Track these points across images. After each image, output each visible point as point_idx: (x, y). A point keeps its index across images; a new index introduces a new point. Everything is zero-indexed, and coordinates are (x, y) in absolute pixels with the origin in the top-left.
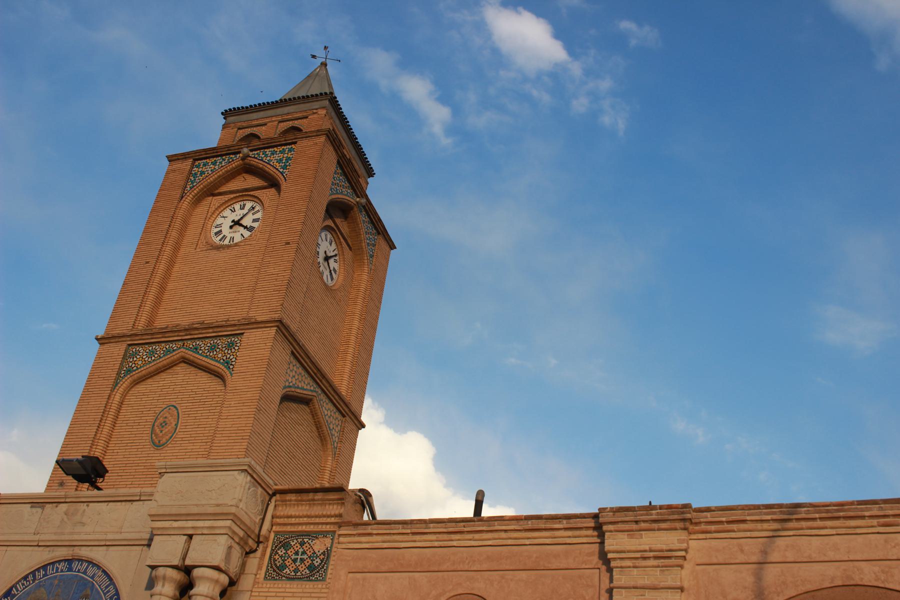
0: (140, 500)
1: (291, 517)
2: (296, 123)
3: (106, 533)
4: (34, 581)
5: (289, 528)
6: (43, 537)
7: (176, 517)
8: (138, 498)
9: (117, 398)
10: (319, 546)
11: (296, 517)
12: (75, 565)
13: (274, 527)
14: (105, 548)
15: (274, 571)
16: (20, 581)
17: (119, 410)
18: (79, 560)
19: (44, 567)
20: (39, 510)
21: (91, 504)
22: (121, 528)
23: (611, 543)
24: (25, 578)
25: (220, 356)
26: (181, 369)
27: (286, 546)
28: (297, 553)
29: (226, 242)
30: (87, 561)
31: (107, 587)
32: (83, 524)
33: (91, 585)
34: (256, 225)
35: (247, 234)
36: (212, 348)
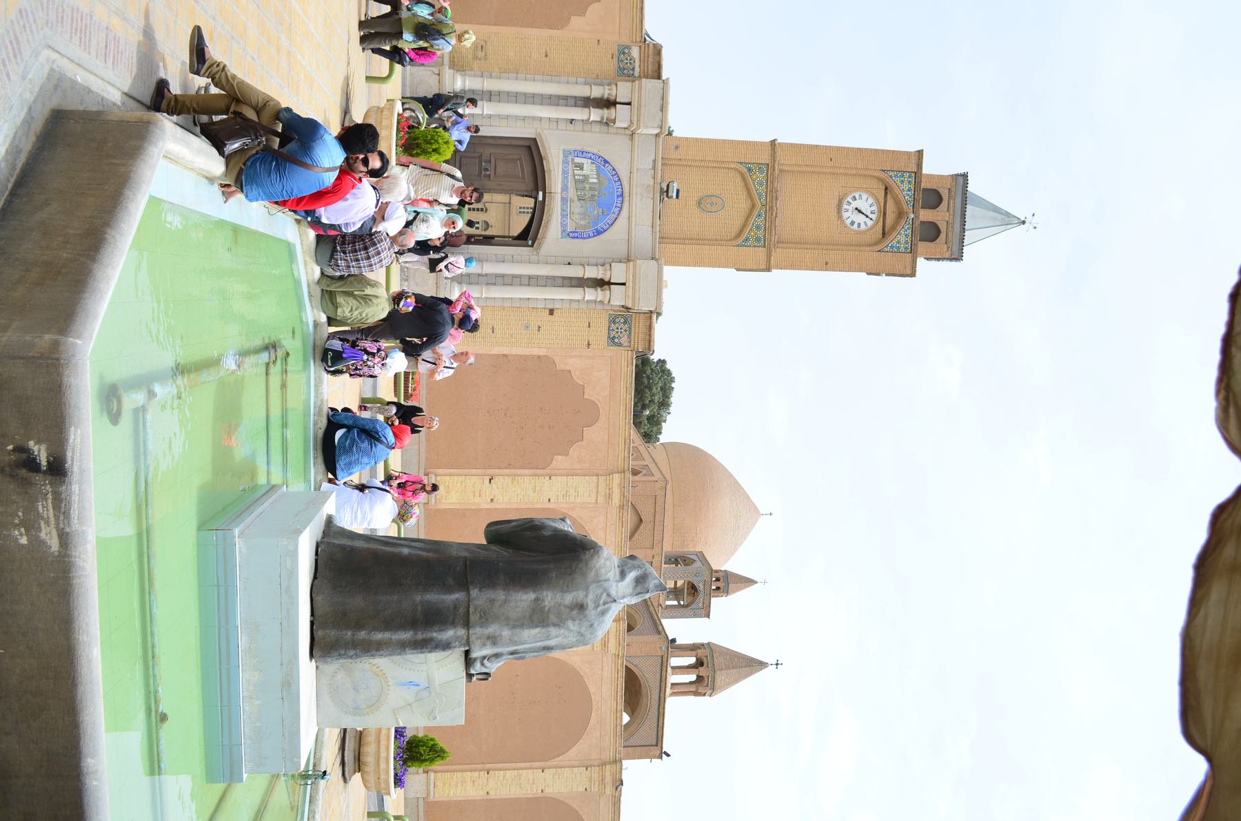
2: (943, 236)
9: (733, 166)
10: (624, 340)
23: (616, 476)
26: (748, 205)
27: (625, 323)
29: (845, 206)
34: (856, 226)
35: (848, 222)
36: (758, 227)
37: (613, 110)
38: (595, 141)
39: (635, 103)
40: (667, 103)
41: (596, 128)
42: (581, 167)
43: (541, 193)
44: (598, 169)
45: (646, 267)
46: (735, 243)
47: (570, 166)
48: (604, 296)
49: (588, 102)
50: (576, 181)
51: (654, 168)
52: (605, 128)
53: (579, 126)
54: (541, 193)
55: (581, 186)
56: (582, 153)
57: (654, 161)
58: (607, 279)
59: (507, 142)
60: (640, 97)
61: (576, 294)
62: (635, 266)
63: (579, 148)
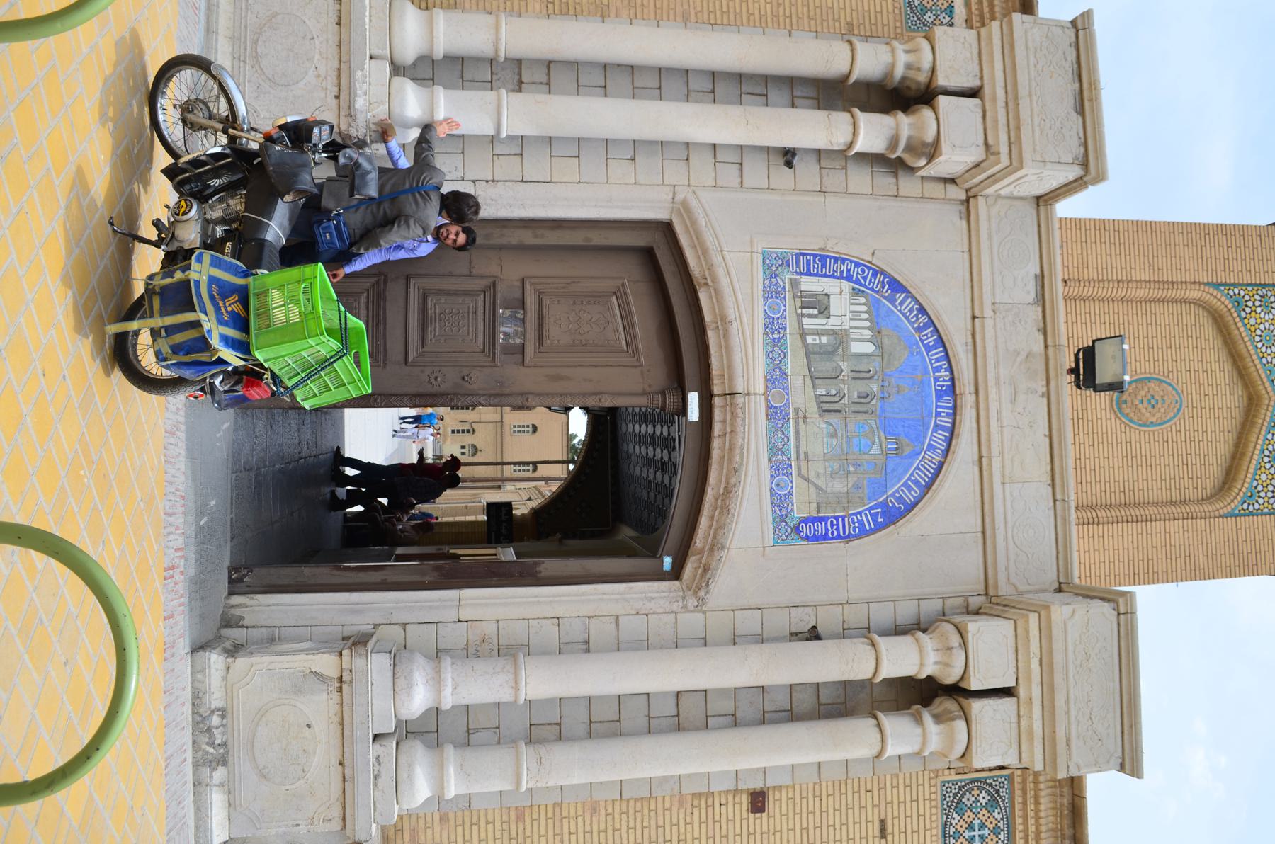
0: (1055, 501)
1: (1037, 803)
3: (1002, 453)
4: (919, 330)
5: (1018, 800)
6: (989, 323)
7: (1047, 663)
8: (1059, 497)
9: (1194, 294)
11: (1037, 811)
12: (947, 402)
13: (1019, 772)
14: (976, 457)
15: (955, 795)
16: (917, 302)
17: (1174, 301)
18: (955, 408)
19: (941, 342)
20: (1031, 297)
21: (1045, 400)
22: (1012, 482)
24: (922, 310)
25: (1264, 477)
28: (982, 826)
30: (954, 424)
31: (916, 483)
32: (1013, 401)
33: (918, 449)
37: (927, 113)
38: (862, 221)
39: (996, 89)
40: (1094, 85)
41: (861, 178)
42: (820, 305)
43: (693, 399)
44: (874, 307)
45: (1078, 623)
46: (1221, 506)
47: (790, 306)
48: (950, 739)
49: (833, 93)
50: (809, 352)
51: (1041, 299)
52: (885, 181)
53: (806, 170)
54: (693, 399)
55: (824, 366)
56: (822, 263)
57: (1041, 279)
58: (950, 678)
59: (576, 238)
60: (1011, 70)
61: (852, 742)
62: (1046, 631)
63: (812, 245)
